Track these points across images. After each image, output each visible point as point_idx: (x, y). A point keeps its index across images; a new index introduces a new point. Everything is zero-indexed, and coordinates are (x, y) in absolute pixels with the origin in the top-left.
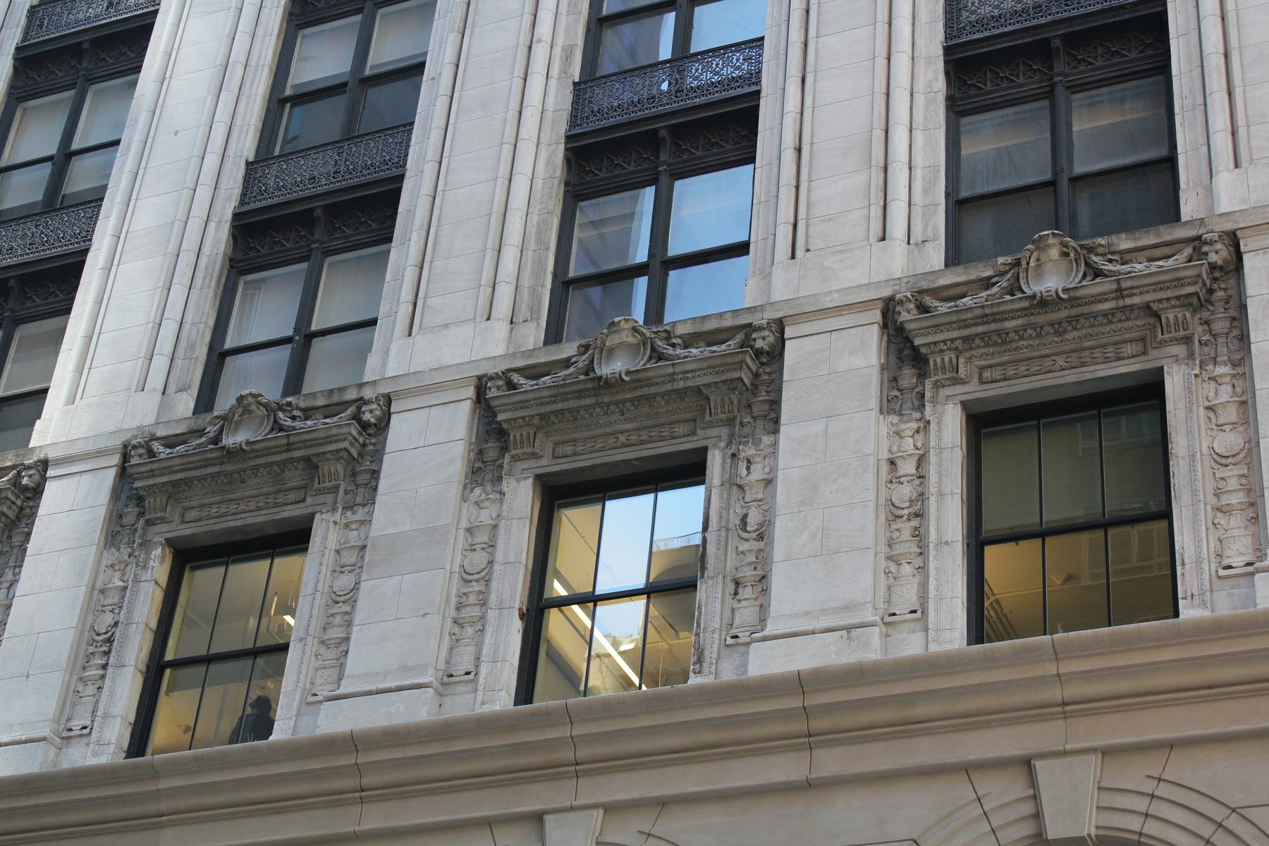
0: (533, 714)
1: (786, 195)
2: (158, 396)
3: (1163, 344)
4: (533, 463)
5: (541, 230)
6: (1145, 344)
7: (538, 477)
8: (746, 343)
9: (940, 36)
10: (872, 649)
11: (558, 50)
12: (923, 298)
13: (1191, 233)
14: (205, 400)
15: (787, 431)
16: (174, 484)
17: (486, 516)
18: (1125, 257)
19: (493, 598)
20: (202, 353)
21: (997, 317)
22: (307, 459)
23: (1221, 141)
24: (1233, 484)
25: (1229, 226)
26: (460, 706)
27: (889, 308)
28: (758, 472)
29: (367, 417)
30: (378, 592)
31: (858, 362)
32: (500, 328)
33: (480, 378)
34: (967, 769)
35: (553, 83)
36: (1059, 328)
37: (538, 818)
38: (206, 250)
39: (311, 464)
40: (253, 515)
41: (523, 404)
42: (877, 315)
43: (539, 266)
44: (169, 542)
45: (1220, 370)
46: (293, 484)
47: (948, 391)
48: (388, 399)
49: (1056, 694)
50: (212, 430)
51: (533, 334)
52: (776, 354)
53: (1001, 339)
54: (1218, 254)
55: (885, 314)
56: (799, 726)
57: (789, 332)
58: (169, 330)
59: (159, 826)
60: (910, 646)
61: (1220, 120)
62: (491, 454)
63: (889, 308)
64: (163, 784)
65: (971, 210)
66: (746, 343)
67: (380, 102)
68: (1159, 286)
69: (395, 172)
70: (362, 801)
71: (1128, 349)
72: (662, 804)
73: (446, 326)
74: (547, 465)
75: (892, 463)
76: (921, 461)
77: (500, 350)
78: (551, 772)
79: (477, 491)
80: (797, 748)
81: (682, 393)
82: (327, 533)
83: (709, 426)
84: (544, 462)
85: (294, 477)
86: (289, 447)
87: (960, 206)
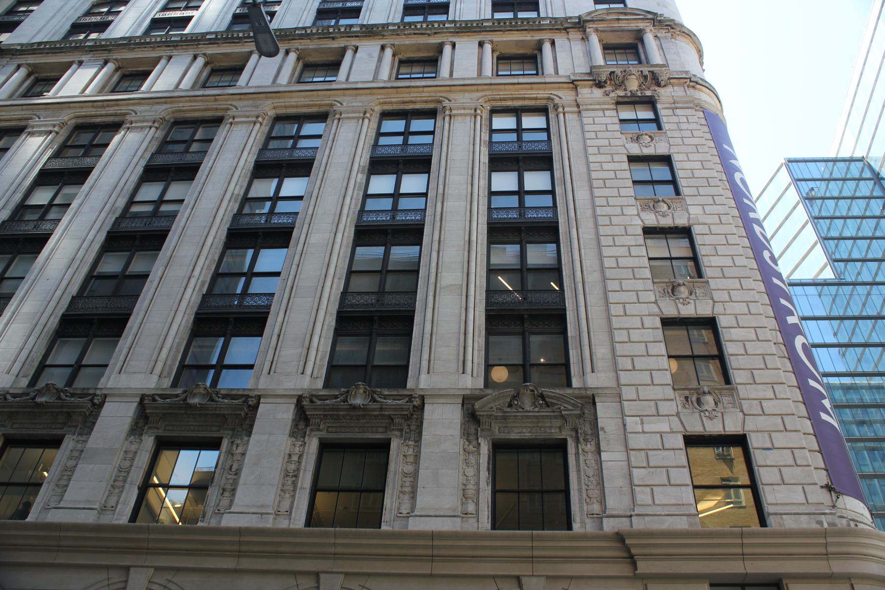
2: (14, 377)
3: (393, 430)
4: (156, 431)
5: (179, 344)
6: (387, 429)
7: (157, 437)
8: (246, 401)
9: (337, 307)
10: (269, 523)
11: (200, 281)
12: (313, 397)
13: (409, 393)
14: (33, 382)
15: (254, 437)
16: (12, 413)
17: (133, 448)
18: (386, 397)
19: (129, 479)
20: (36, 364)
21: (338, 410)
22: (68, 413)
23: (425, 363)
24: (408, 484)
25: (422, 393)
26: (107, 519)
27: (300, 399)
28: (240, 450)
29: (96, 401)
30: (84, 468)
31: (285, 416)
32: (155, 378)
33: (143, 395)
35: (195, 293)
37: (127, 569)
38: (48, 325)
39: (69, 415)
40: (40, 431)
41: (156, 408)
42: (295, 401)
43: (175, 357)
45: (410, 443)
47: (315, 433)
48: (105, 396)
49: (332, 550)
50: (32, 394)
51: (167, 383)
52: (256, 408)
54: (417, 402)
55: (298, 401)
56: (236, 548)
57: (262, 400)
58: (25, 353)
60: (283, 524)
61: (425, 356)
62: (141, 425)
63: (300, 399)
65: (336, 370)
66: (246, 401)
67: (129, 286)
68: (395, 409)
69: (129, 312)
70: (58, 551)
71: (381, 430)
72: (178, 570)
73: (135, 373)
74: (161, 432)
75: (290, 455)
76: (300, 456)
77: (153, 386)
79: (132, 437)
81: (218, 415)
82: (69, 443)
84: (160, 431)
86: (62, 407)
87: (332, 367)
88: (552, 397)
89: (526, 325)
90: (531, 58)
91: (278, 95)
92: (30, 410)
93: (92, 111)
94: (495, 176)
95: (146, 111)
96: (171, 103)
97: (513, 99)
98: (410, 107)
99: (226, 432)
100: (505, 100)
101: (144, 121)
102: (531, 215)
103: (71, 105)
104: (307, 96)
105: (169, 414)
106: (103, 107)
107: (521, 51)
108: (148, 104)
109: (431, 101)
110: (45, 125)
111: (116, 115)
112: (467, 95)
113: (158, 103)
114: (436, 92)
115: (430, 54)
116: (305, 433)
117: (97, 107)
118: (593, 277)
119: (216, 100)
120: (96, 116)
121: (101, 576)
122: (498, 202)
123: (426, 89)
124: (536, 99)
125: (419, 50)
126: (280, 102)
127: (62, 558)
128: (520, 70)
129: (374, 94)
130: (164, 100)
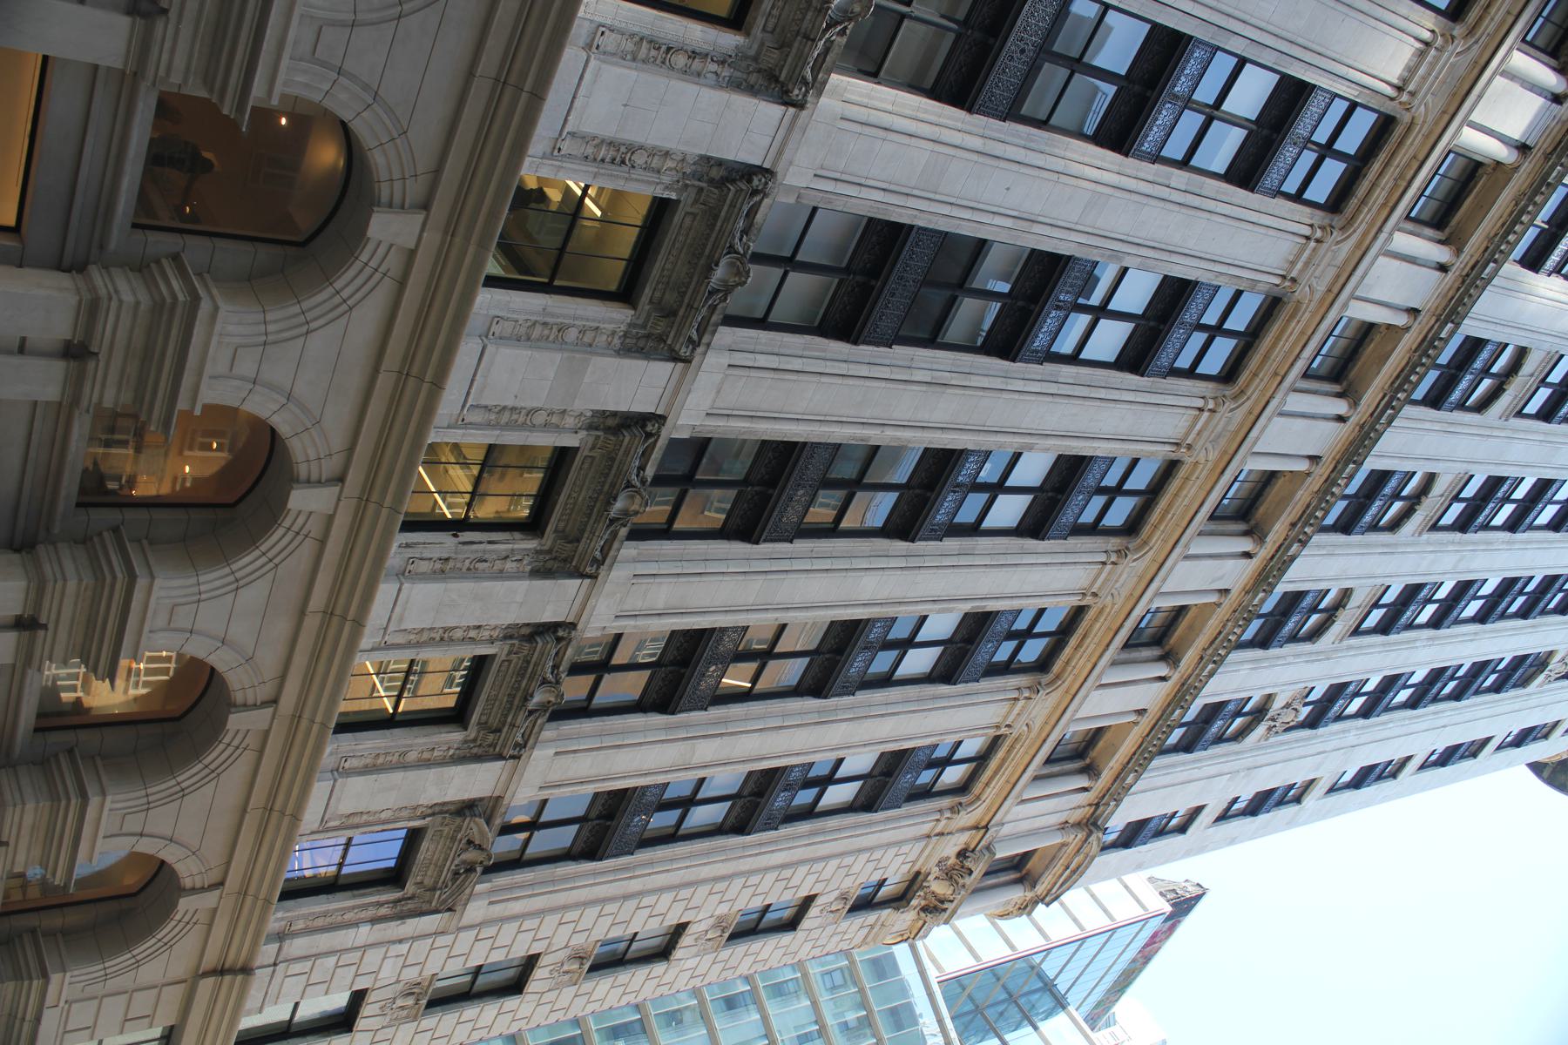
0: (476, 282)
1: (773, 362)
6: (482, 725)
16: (716, 217)
22: (675, 314)
34: (283, 678)
36: (512, 696)
39: (670, 314)
44: (678, 202)
46: (667, 296)
48: (687, 361)
49: (306, 715)
53: (521, 673)
54: (796, 93)
55: (767, 170)
56: (338, 611)
59: (446, 233)
63: (768, 173)
64: (472, 249)
78: (364, 500)
80: (327, 606)
81: (582, 531)
83: (555, 541)
85: (671, 298)
86: (690, 307)
88: (464, 881)
89: (858, 278)
90: (1443, 218)
91: (1219, 470)
92: (707, 251)
93: (1402, 158)
94: (1268, 81)
95: (1334, 258)
96: (1323, 299)
97: (1004, 760)
98: (1073, 642)
99: (755, 46)
100: (1009, 752)
101: (1307, 264)
102: (1164, 115)
103: (1447, 117)
104: (1186, 511)
105: (611, 467)
106: (1401, 176)
107: (1101, 744)
108: (1347, 261)
109: (1064, 670)
110: (1424, 79)
111: (1363, 202)
112: (1046, 712)
113: (1338, 276)
114: (1076, 676)
115: (1352, 375)
116: (597, 429)
117: (1408, 165)
118: (635, 885)
119: (1276, 374)
120: (1387, 164)
121: (338, 441)
122: (1221, 66)
123: (1089, 666)
124: (987, 784)
125: (1191, 627)
126: (1202, 473)
127: (385, 382)
128: (1434, 191)
129: (1128, 598)
130: (1335, 290)
